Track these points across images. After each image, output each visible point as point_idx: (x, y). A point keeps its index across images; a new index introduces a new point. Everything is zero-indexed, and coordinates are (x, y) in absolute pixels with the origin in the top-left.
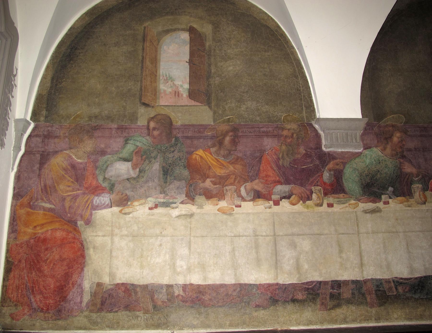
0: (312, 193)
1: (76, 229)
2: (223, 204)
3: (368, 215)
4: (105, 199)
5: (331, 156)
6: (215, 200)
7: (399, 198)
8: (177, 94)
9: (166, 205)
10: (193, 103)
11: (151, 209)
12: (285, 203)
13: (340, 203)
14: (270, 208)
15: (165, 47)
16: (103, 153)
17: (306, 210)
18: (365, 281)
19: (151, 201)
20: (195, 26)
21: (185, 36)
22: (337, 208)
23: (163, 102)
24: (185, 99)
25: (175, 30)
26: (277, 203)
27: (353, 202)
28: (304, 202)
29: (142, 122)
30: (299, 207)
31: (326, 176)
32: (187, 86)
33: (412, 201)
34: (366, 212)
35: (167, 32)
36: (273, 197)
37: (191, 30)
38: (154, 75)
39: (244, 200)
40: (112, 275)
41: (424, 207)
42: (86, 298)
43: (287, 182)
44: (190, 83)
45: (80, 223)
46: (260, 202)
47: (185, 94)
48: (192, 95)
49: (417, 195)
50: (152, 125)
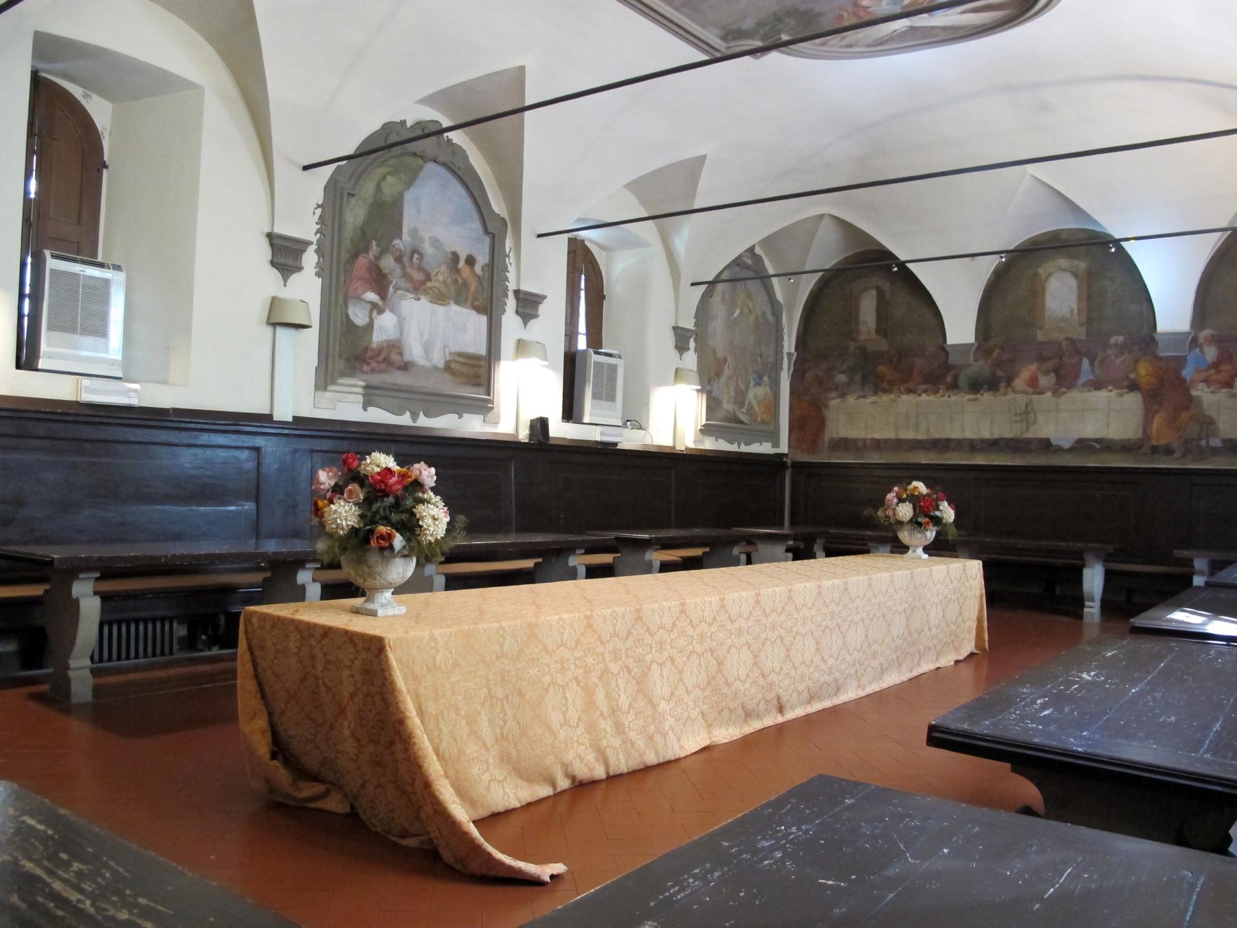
0: (939, 389)
1: (821, 412)
2: (892, 396)
3: (970, 403)
4: (834, 394)
5: (953, 367)
6: (887, 394)
7: (991, 392)
8: (869, 332)
9: (864, 397)
10: (878, 337)
11: (856, 399)
12: (924, 397)
13: (955, 395)
14: (915, 398)
15: (862, 301)
16: (832, 369)
17: (935, 399)
18: (964, 439)
19: (856, 395)
20: (879, 284)
21: (874, 292)
22: (953, 398)
23: (862, 337)
24: (873, 335)
25: (869, 288)
26: (920, 395)
27: (962, 394)
28: (935, 394)
29: (851, 349)
30: (932, 398)
31: (949, 379)
32: (875, 327)
33: (998, 394)
34: (969, 400)
35: (865, 289)
36: (919, 392)
37: (878, 289)
38: (857, 319)
39: (902, 394)
40: (837, 433)
41: (1005, 398)
42: (826, 445)
43: (926, 381)
44: (877, 324)
45: (822, 408)
46: (911, 394)
47: (874, 332)
48: (878, 331)
49: (1002, 389)
50: (856, 352)
